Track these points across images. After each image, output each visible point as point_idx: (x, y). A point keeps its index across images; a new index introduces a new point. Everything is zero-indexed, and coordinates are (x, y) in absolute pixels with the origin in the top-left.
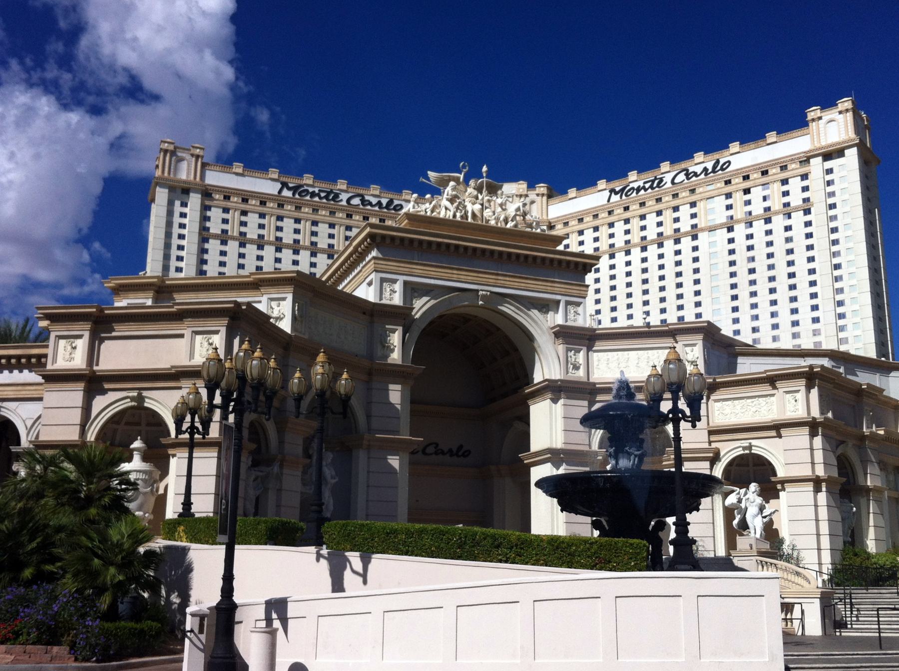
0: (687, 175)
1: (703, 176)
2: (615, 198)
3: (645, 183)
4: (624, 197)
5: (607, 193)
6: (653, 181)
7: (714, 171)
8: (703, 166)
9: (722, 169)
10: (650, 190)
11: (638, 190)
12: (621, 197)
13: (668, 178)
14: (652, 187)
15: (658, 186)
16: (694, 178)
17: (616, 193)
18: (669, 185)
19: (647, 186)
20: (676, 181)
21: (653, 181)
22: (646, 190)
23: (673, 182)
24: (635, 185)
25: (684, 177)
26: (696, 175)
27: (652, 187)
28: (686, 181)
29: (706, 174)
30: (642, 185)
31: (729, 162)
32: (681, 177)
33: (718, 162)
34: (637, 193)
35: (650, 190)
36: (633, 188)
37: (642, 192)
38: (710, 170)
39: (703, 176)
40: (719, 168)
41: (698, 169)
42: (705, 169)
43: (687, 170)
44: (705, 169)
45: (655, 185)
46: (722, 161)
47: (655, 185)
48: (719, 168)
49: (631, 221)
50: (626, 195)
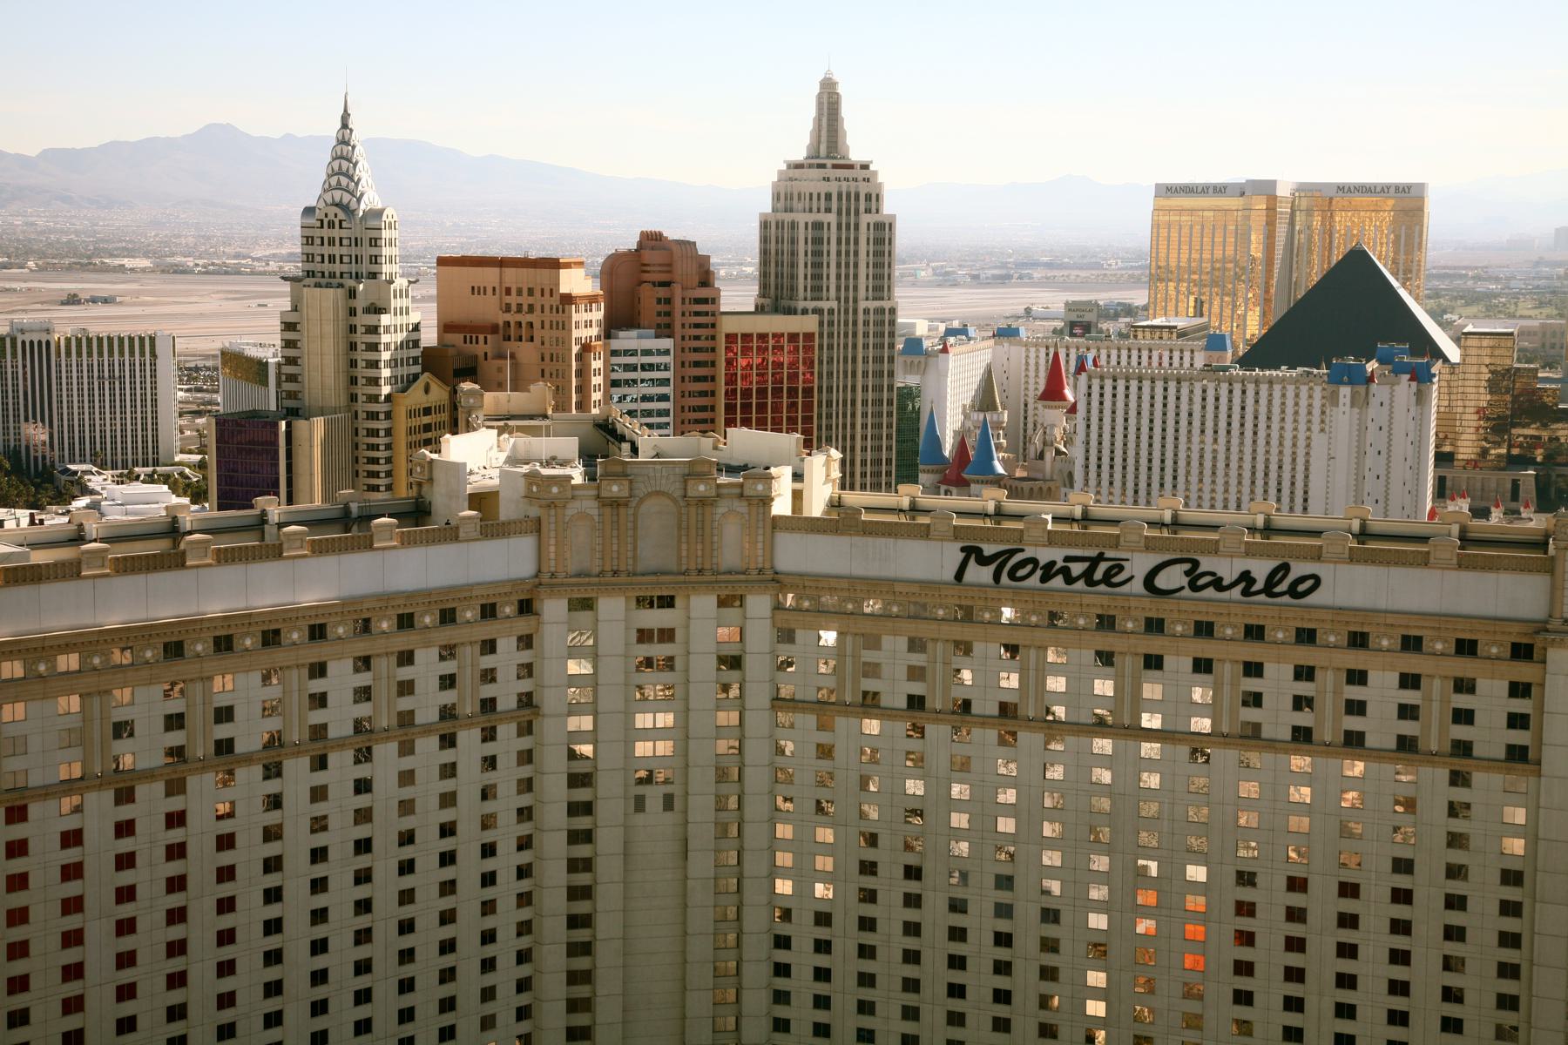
0: (1195, 578)
1: (1236, 593)
2: (979, 574)
3: (1068, 559)
4: (1005, 579)
5: (952, 555)
6: (1095, 562)
7: (1269, 589)
8: (1240, 565)
9: (1293, 592)
10: (1080, 585)
11: (1049, 572)
12: (997, 577)
13: (1138, 566)
14: (1088, 576)
15: (1107, 579)
16: (1210, 592)
17: (983, 561)
18: (1137, 586)
19: (1077, 569)
20: (1161, 582)
21: (1095, 562)
22: (1070, 580)
23: (1149, 581)
24: (1045, 555)
25: (1185, 581)
26: (1218, 584)
27: (1088, 576)
28: (1187, 592)
29: (1246, 593)
30: (1060, 564)
31: (1317, 581)
32: (1173, 578)
33: (1285, 568)
34: (1044, 579)
35: (1080, 585)
36: (1034, 561)
37: (1058, 582)
38: (1259, 585)
39: (1236, 593)
40: (1283, 587)
41: (1229, 570)
42: (1246, 578)
43: (1196, 564)
44: (1246, 578)
45: (1098, 575)
46: (1299, 569)
47: (1098, 575)
48: (1283, 587)
49: (1448, 748)
50: (1012, 576)
